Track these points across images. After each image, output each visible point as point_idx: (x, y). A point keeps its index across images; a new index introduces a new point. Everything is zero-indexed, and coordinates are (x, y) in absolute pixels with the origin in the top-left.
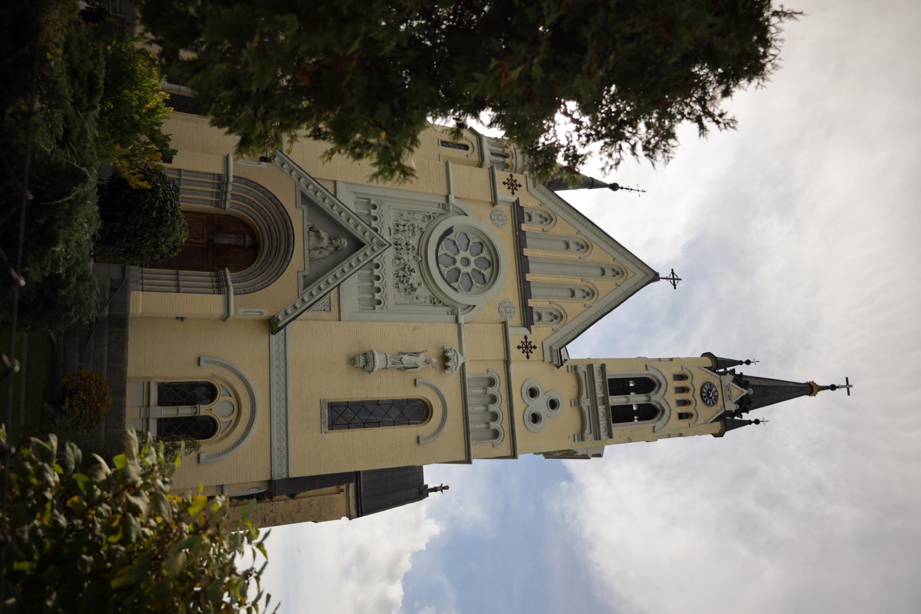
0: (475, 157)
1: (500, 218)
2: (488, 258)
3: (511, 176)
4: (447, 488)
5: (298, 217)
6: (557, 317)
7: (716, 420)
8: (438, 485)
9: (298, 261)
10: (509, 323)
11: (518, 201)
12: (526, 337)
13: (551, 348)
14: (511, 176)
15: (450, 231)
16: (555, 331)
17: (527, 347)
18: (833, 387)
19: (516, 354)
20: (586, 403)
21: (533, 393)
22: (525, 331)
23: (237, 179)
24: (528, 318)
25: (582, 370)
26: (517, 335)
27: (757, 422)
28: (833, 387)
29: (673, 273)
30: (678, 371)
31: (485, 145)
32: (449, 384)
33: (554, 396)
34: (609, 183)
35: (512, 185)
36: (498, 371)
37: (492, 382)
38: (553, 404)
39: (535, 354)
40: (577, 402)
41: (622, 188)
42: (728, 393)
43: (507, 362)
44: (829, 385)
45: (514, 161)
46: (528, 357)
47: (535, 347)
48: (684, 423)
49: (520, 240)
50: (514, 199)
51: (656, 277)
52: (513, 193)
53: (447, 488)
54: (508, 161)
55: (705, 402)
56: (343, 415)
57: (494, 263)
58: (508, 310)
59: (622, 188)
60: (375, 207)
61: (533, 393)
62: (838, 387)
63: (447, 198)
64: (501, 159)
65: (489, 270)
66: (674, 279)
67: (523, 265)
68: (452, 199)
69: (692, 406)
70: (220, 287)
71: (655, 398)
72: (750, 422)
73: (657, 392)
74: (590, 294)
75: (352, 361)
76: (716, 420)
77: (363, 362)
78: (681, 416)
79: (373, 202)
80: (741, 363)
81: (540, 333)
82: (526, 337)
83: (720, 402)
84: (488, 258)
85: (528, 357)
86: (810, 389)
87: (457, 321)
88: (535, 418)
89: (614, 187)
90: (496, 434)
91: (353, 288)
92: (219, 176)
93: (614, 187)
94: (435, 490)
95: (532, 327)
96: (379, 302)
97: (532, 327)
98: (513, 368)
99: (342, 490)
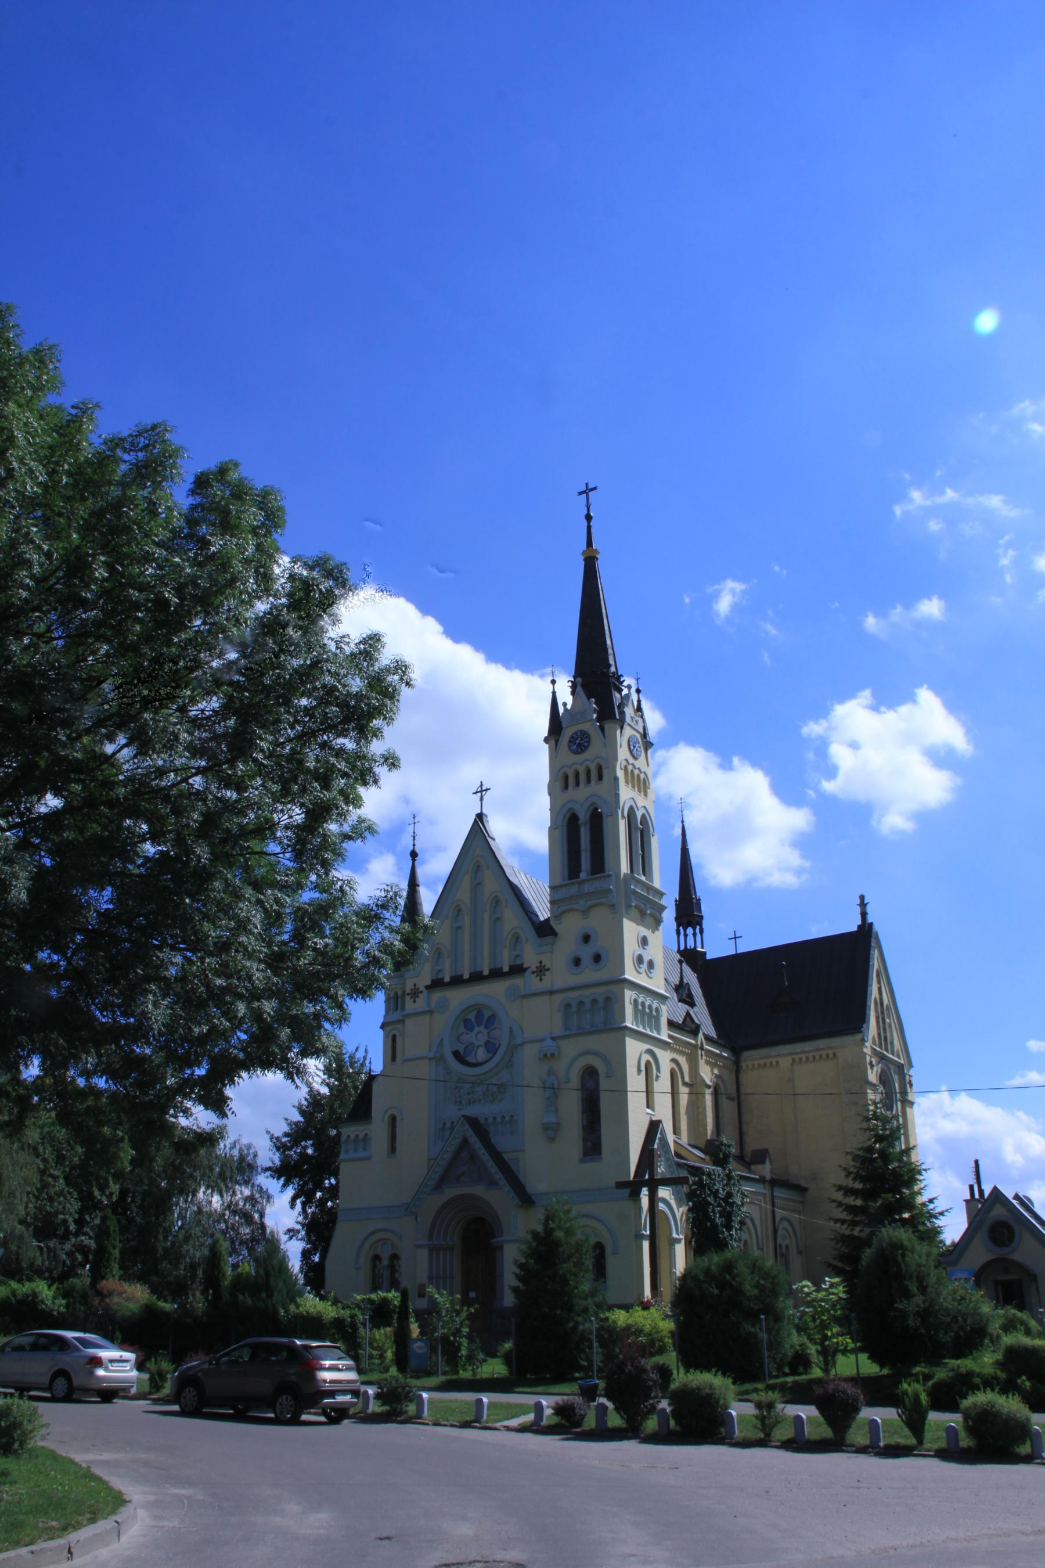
0: (400, 1026)
4: (862, 897)
5: (451, 1192)
6: (517, 939)
7: (602, 728)
8: (858, 910)
9: (479, 1190)
11: (427, 987)
12: (533, 972)
13: (540, 946)
15: (456, 1054)
17: (541, 971)
19: (546, 983)
21: (577, 962)
22: (528, 972)
23: (430, 1237)
24: (517, 970)
26: (530, 982)
28: (589, 518)
29: (476, 793)
30: (559, 785)
31: (389, 1019)
32: (570, 1048)
34: (411, 862)
35: (415, 993)
36: (558, 999)
37: (568, 1006)
38: (587, 939)
39: (547, 963)
40: (585, 912)
43: (552, 992)
44: (585, 523)
46: (548, 970)
47: (541, 962)
48: (605, 772)
49: (457, 981)
50: (425, 992)
51: (480, 817)
53: (862, 897)
54: (400, 993)
55: (586, 748)
56: (592, 1147)
60: (444, 1124)
61: (577, 962)
63: (430, 1059)
66: (482, 791)
67: (477, 977)
68: (431, 1055)
70: (500, 1248)
71: (583, 816)
74: (497, 902)
75: (552, 1139)
76: (602, 728)
77: (551, 1131)
78: (600, 777)
79: (441, 1126)
80: (554, 693)
81: (530, 958)
82: (533, 972)
83: (586, 727)
85: (548, 970)
87: (522, 1045)
88: (597, 958)
90: (608, 999)
91: (502, 1142)
92: (431, 1251)
94: (864, 915)
95: (525, 966)
96: (512, 1116)
97: (525, 966)
98: (558, 985)
99: (834, 1054)
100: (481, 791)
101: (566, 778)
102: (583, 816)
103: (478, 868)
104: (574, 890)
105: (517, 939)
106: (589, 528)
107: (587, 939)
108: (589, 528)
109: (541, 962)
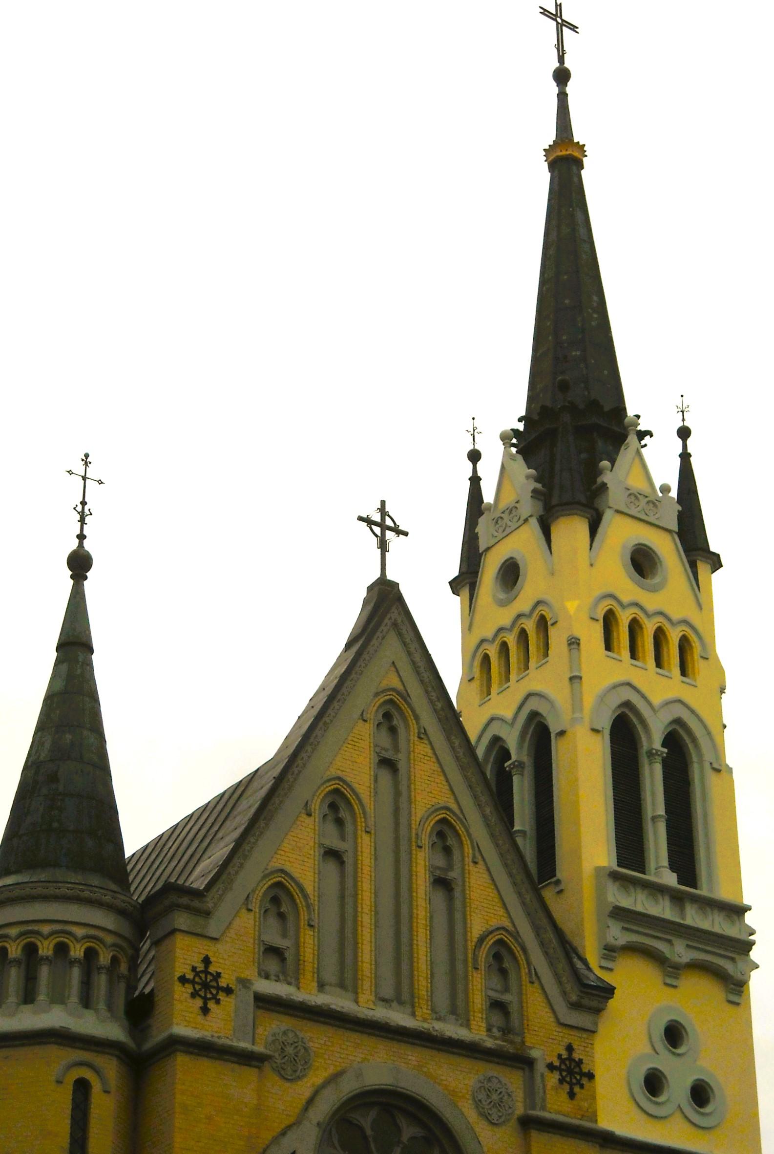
1: (290, 1050)
2: (373, 1114)
3: (183, 980)
7: (693, 565)
10: (520, 1110)
14: (183, 980)
16: (535, 977)
18: (562, 76)
20: (680, 951)
21: (654, 1083)
25: (617, 935)
27: (684, 433)
28: (562, 76)
30: (598, 630)
33: (659, 1032)
38: (674, 1034)
40: (671, 970)
41: (81, 537)
42: (644, 501)
45: (109, 939)
48: (700, 666)
52: (228, 991)
54: (104, 958)
57: (392, 1103)
58: (495, 1097)
59: (81, 537)
61: (654, 1083)
62: (561, 59)
64: (101, 981)
65: (402, 1122)
69: (667, 627)
71: (654, 738)
72: (685, 457)
73: (643, 722)
74: (445, 833)
76: (693, 565)
84: (373, 1114)
86: (566, 163)
88: (700, 1094)
89: (80, 564)
93: (80, 564)
100: (382, 525)
101: (609, 621)
102: (654, 738)
103: (390, 716)
104: (640, 902)
105: (502, 955)
106: (563, 97)
107: (674, 1034)
108: (563, 97)
109: (570, 1048)
